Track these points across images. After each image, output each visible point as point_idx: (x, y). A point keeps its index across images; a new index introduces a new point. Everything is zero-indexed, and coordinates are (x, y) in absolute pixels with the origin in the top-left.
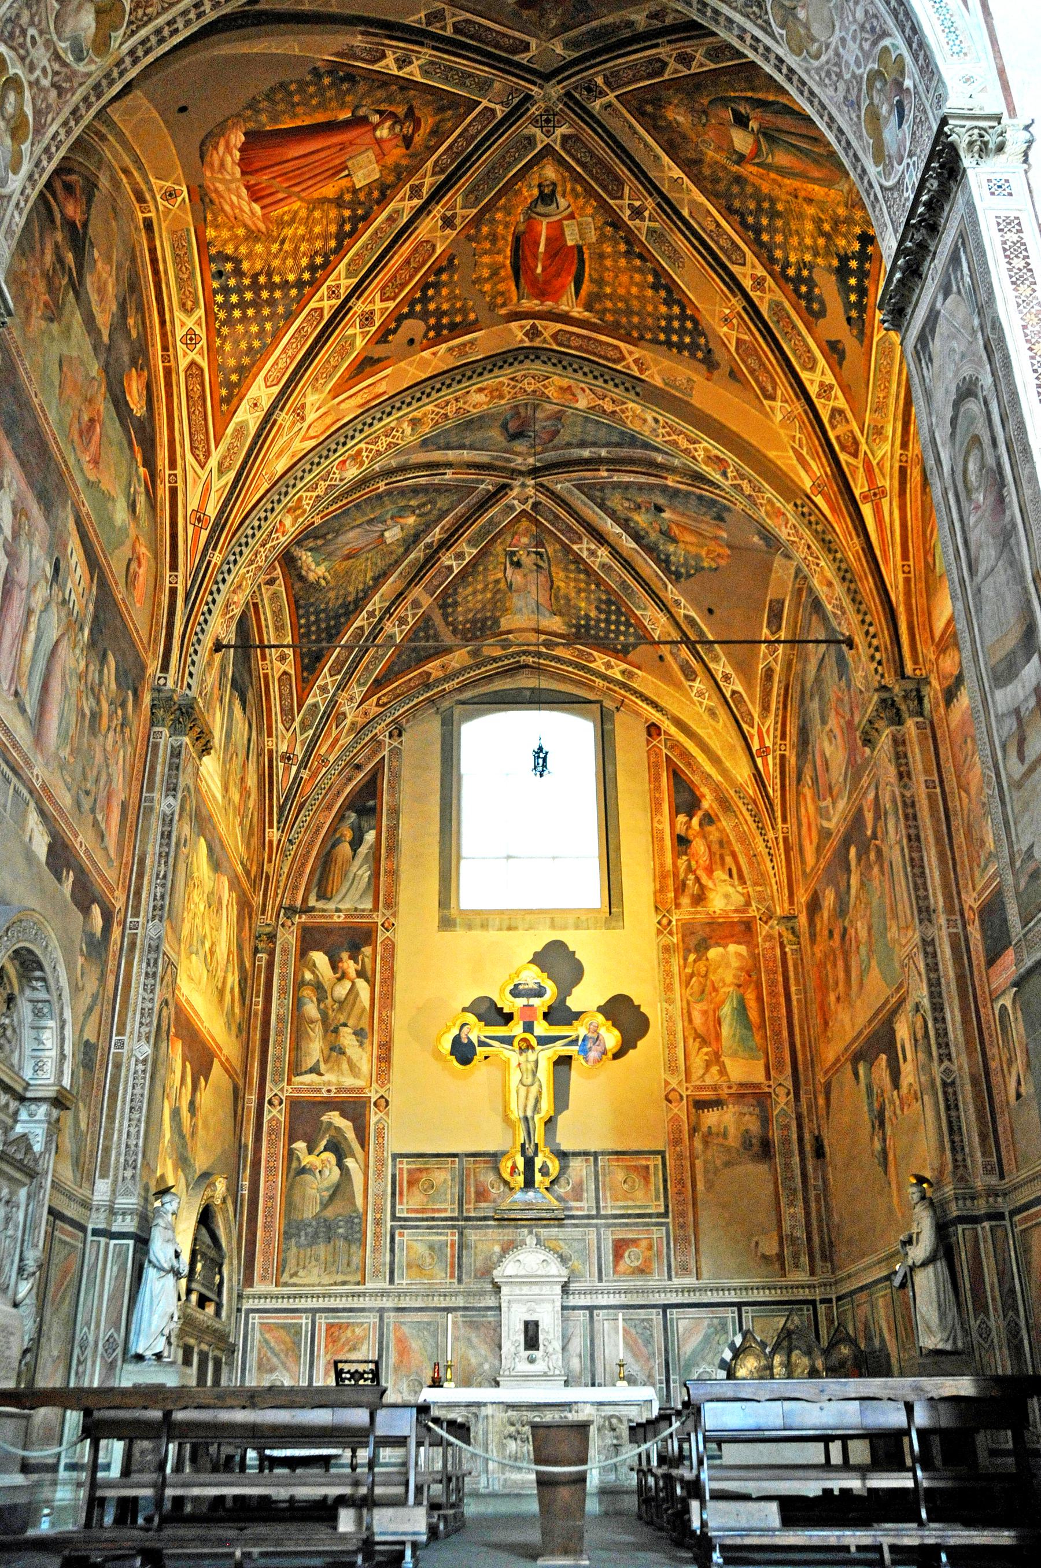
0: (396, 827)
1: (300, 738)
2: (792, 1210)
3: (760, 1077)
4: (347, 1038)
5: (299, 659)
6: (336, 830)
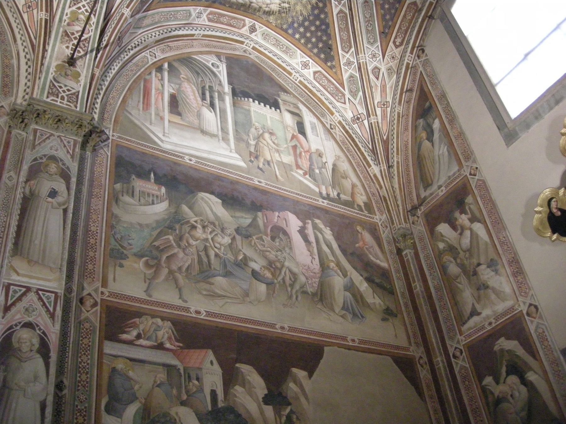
0: (448, 104)
1: (356, 102)
4: (485, 274)
5: (317, 59)
6: (416, 138)
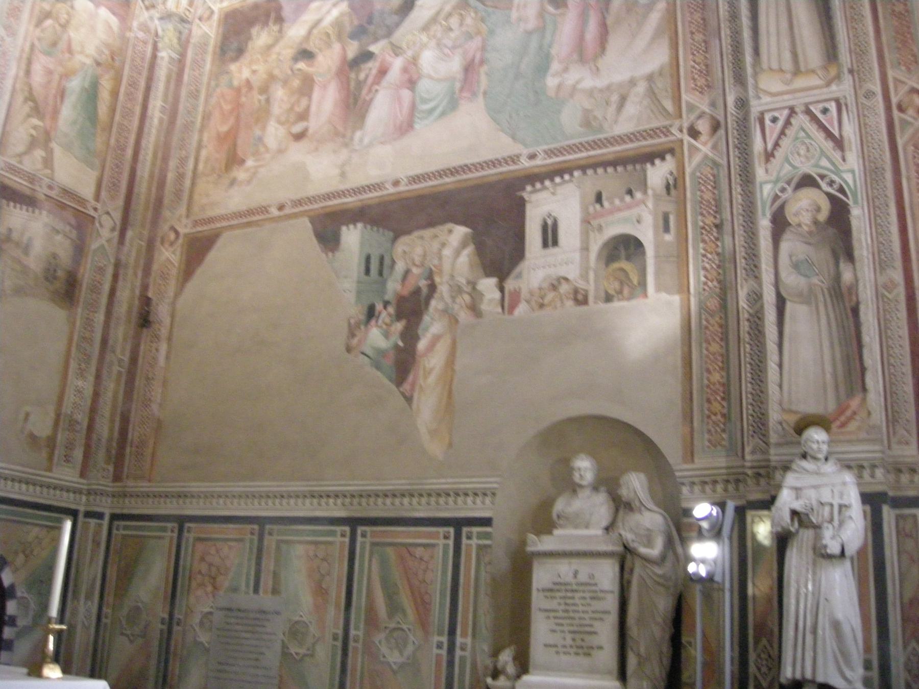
2: (80, 383)
3: (87, 192)
